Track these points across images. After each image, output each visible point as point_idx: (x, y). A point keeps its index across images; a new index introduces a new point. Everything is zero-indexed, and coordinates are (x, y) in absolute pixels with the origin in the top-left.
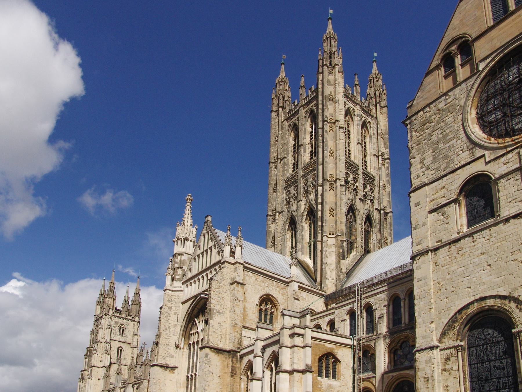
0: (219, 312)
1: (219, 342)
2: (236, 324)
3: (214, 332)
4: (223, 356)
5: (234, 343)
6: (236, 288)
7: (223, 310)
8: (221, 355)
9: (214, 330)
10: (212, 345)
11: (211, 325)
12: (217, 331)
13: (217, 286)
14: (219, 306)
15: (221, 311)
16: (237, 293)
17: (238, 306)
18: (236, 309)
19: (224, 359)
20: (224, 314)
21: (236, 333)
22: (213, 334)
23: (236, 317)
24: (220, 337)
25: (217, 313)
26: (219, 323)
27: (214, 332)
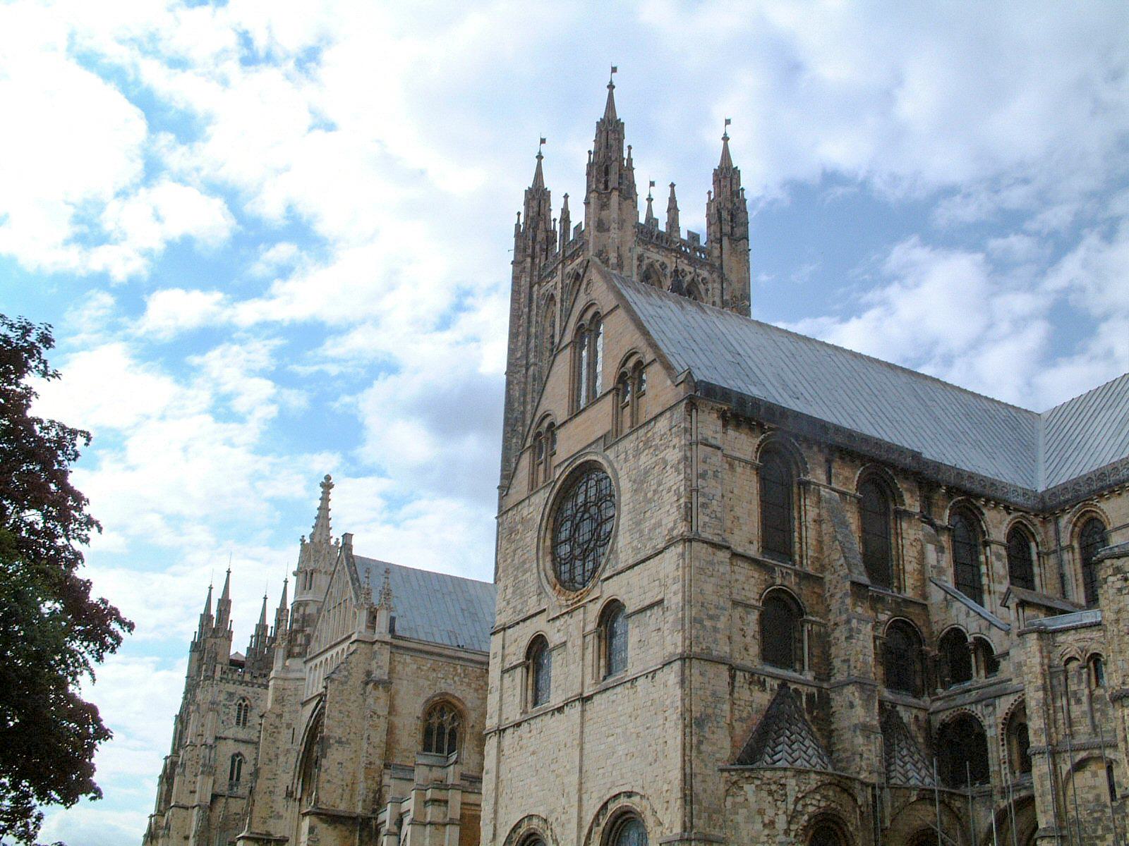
0: (340, 742)
1: (338, 801)
2: (370, 763)
3: (329, 781)
4: (344, 828)
5: (364, 801)
6: (373, 692)
7: (348, 737)
8: (340, 827)
9: (329, 778)
10: (324, 807)
11: (323, 769)
12: (335, 780)
13: (337, 693)
14: (341, 729)
15: (344, 739)
16: (375, 703)
17: (375, 727)
18: (373, 734)
19: (347, 833)
20: (350, 744)
21: (370, 782)
22: (327, 786)
23: (371, 751)
24: (340, 791)
25: (336, 745)
26: (339, 763)
27: (329, 781)
